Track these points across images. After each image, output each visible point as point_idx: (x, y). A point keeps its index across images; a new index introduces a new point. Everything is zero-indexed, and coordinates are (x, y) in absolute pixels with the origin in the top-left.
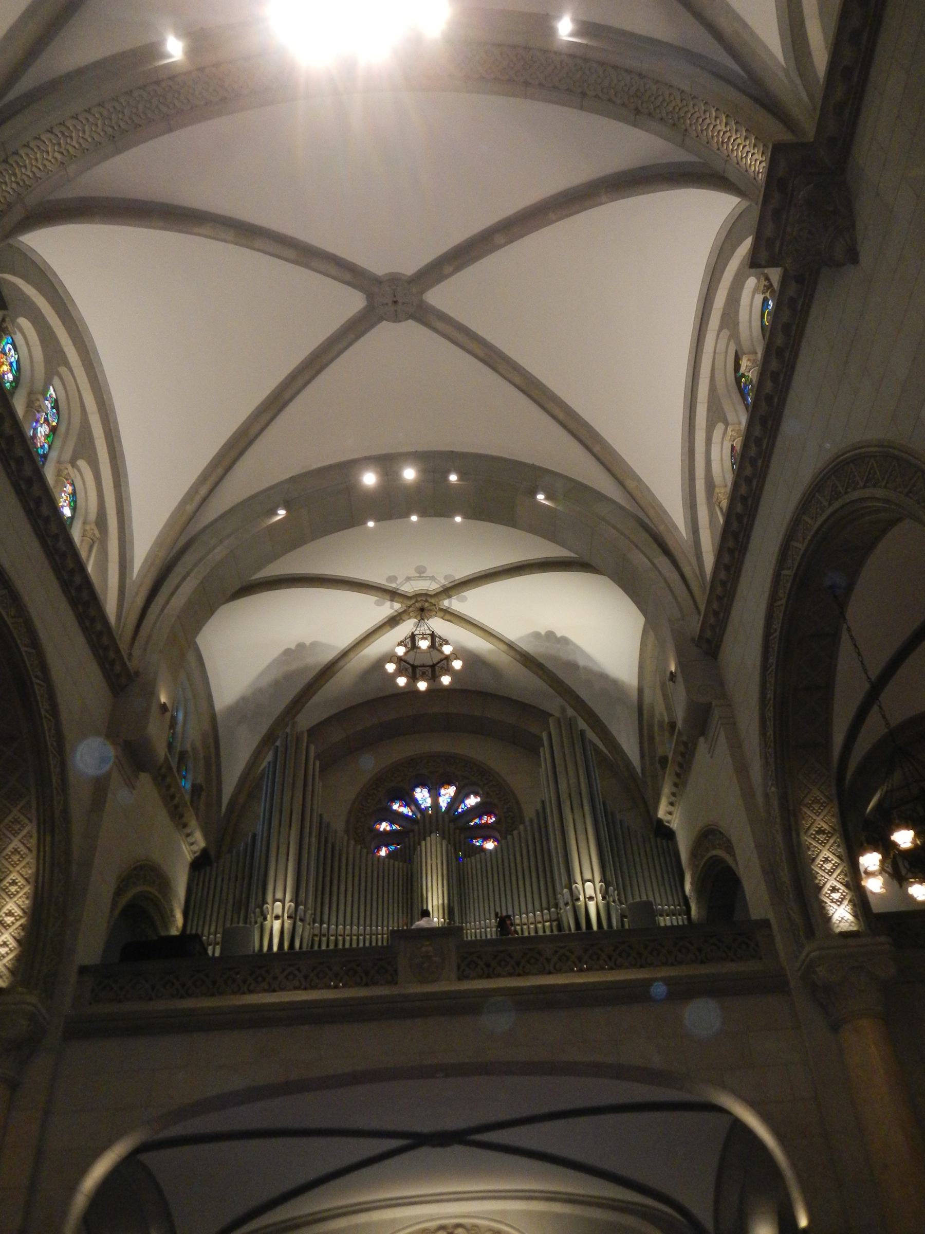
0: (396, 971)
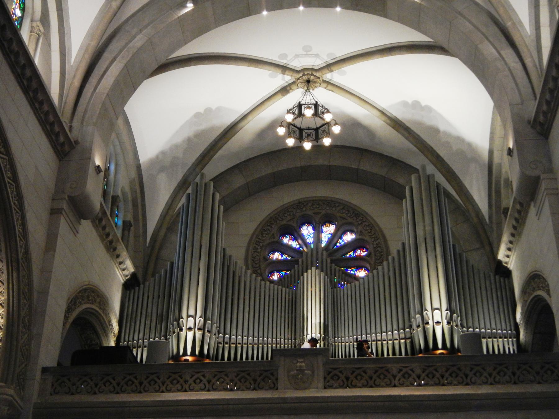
0: (277, 379)
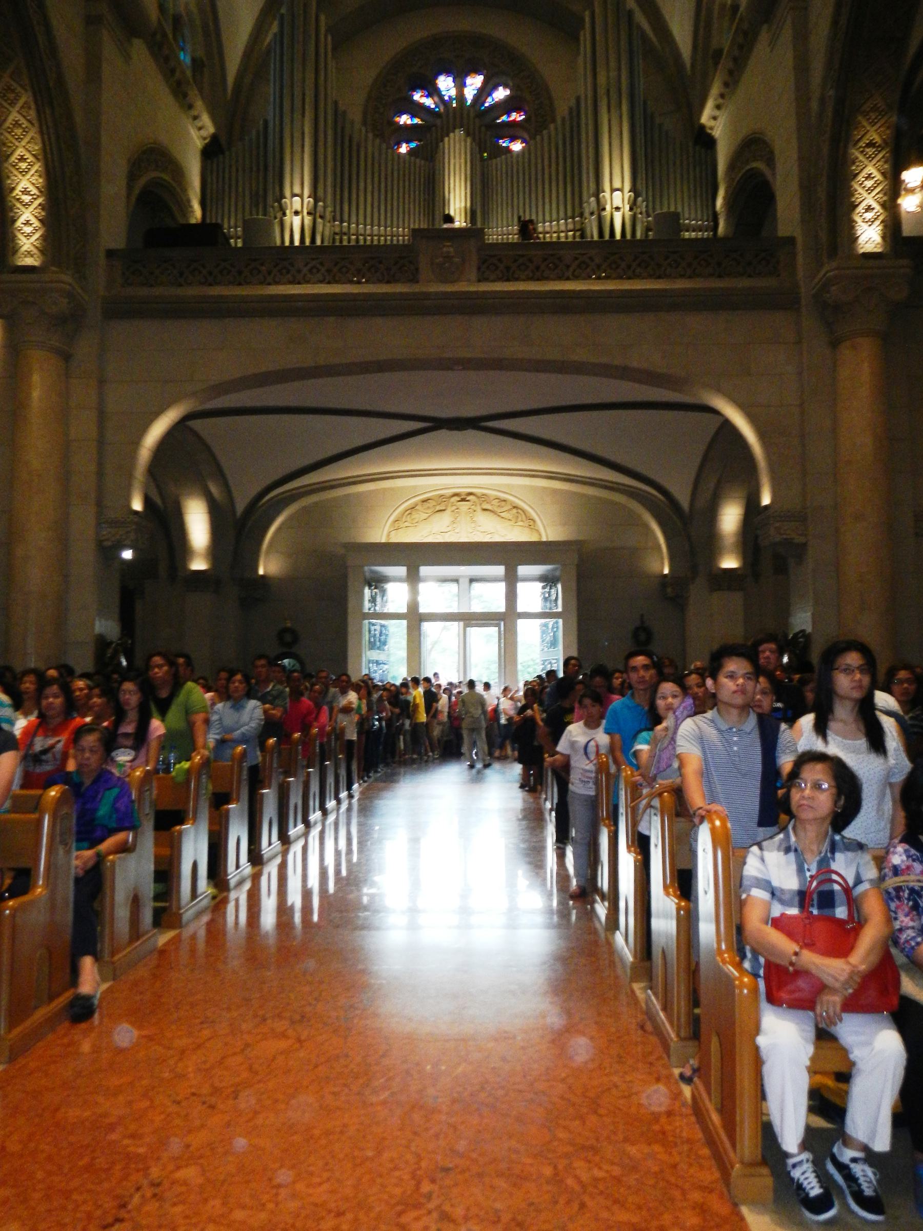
0: (417, 269)
